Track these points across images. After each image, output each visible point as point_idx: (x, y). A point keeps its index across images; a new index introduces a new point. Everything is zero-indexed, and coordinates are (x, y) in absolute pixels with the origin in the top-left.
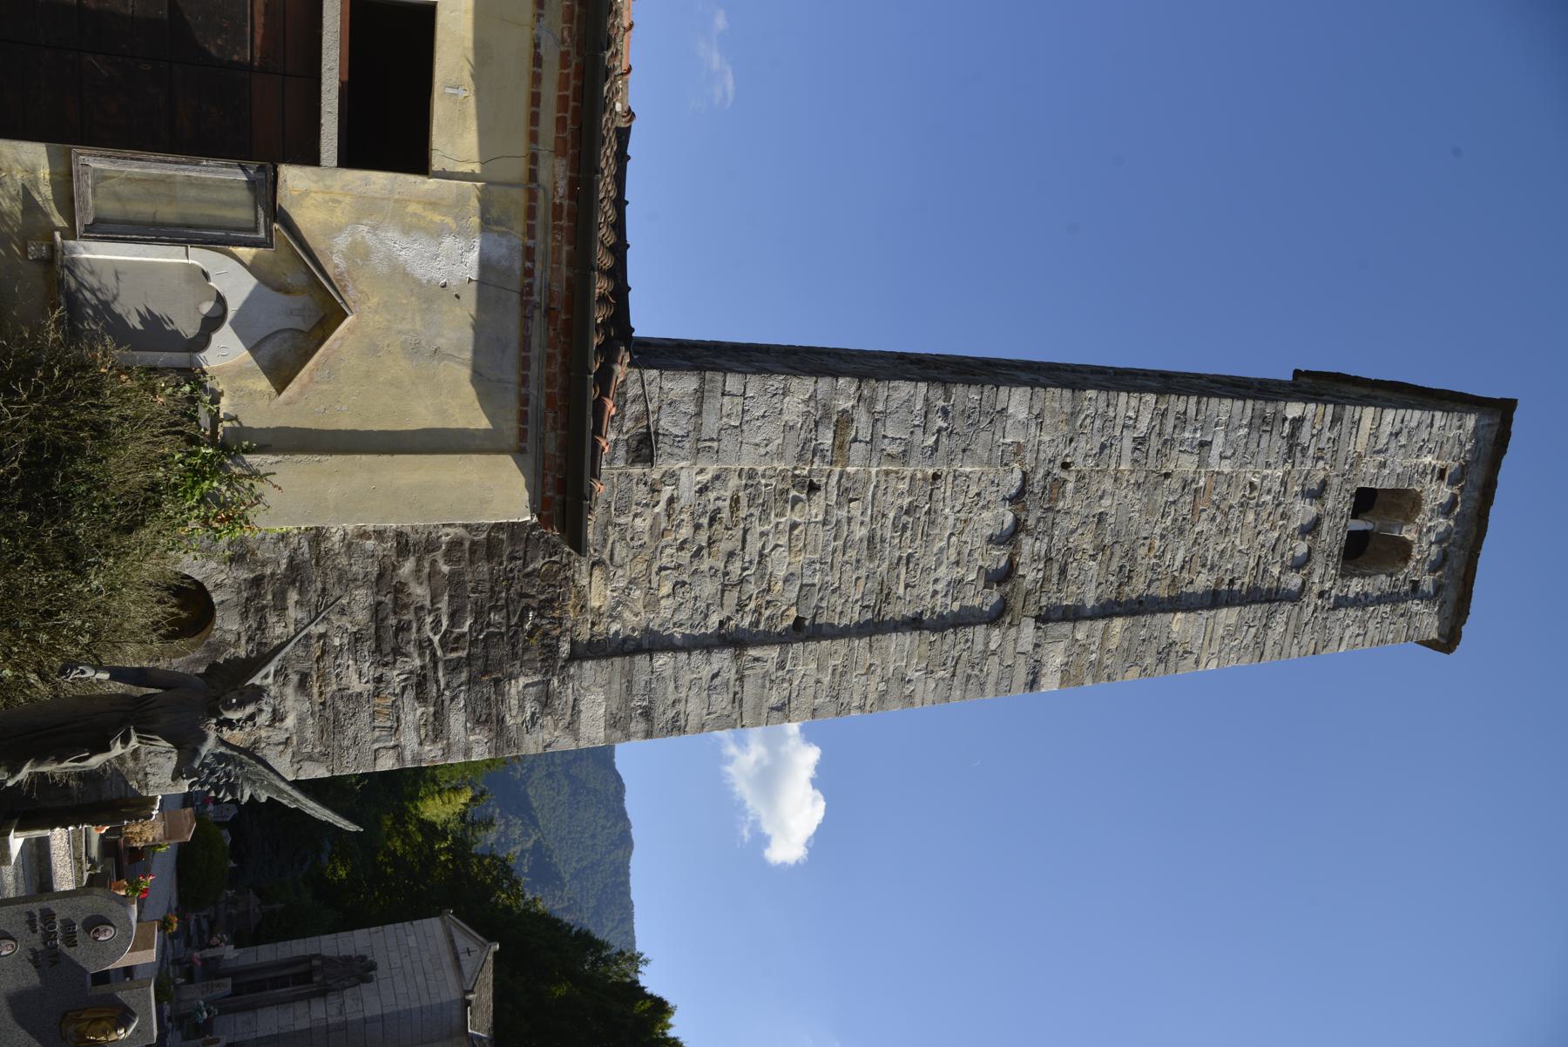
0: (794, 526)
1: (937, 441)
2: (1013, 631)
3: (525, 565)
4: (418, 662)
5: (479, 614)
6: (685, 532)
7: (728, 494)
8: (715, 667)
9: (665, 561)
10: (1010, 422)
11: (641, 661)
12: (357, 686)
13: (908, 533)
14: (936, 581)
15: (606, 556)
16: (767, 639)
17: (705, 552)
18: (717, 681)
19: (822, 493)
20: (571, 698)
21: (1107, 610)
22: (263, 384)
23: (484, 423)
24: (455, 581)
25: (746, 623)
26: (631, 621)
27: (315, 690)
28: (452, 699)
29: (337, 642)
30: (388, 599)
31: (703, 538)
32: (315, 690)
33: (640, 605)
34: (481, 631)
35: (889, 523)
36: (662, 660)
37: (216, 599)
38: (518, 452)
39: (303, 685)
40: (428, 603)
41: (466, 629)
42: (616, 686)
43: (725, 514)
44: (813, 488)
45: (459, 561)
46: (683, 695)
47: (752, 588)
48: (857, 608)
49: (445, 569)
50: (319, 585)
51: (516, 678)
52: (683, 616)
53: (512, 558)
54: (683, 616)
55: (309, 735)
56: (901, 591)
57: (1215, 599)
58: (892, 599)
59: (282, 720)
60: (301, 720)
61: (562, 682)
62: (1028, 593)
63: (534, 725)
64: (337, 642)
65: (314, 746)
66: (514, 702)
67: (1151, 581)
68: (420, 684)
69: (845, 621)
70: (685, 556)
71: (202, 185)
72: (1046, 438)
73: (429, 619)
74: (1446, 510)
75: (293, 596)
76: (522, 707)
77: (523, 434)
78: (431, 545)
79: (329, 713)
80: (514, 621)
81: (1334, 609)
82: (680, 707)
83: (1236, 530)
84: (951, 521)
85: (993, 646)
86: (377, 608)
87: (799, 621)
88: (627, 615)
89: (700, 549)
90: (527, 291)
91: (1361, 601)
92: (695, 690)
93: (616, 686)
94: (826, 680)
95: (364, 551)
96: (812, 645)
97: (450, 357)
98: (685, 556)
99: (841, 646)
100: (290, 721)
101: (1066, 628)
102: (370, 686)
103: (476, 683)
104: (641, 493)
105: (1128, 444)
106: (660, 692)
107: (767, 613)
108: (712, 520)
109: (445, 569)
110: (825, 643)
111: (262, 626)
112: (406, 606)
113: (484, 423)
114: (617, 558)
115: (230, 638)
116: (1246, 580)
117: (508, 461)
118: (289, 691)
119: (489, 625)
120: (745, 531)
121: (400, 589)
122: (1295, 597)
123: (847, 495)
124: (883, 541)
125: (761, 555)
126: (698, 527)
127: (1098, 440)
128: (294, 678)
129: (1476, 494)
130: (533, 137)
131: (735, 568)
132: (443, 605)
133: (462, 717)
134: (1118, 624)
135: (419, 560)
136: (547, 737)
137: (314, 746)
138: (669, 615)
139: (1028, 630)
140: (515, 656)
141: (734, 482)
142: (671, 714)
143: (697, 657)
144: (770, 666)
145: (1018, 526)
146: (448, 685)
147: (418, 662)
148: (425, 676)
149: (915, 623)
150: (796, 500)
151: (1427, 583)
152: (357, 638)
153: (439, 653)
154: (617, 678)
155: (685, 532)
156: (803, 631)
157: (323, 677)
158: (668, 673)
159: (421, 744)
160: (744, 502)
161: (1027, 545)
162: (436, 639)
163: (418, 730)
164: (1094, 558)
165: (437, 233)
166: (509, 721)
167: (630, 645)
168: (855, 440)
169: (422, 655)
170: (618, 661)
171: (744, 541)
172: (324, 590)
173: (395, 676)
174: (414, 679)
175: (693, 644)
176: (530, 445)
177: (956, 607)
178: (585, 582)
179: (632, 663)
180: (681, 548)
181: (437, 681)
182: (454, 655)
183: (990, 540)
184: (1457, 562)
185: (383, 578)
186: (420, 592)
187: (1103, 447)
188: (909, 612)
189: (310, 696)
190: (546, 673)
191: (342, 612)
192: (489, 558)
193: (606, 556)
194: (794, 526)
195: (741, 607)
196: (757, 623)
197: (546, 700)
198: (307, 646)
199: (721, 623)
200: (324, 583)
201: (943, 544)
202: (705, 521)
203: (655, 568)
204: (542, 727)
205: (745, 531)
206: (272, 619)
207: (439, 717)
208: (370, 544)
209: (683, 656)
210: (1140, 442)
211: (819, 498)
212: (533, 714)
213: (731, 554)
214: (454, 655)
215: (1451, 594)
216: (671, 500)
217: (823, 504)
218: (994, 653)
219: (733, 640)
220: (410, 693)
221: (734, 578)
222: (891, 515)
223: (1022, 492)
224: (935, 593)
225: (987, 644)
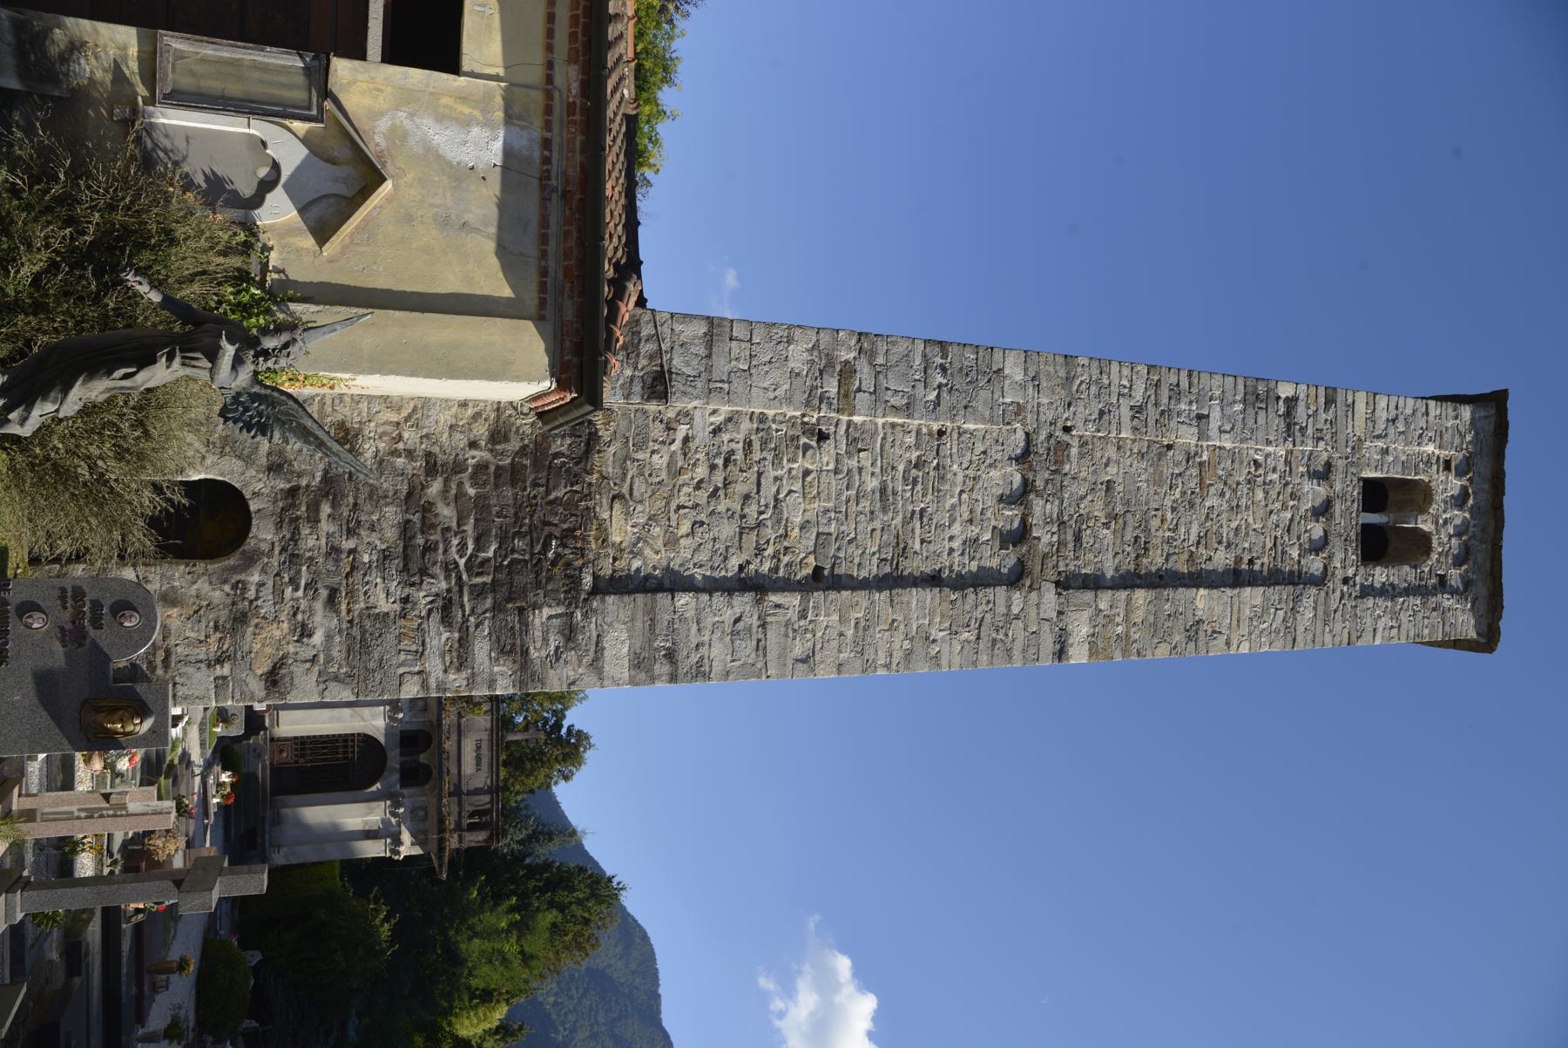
0: (807, 473)
1: (938, 396)
2: (1034, 594)
3: (548, 492)
4: (444, 585)
5: (503, 539)
6: (701, 471)
7: (741, 437)
8: (738, 611)
9: (683, 500)
10: (1007, 382)
11: (663, 599)
12: (384, 605)
13: (919, 487)
14: (951, 538)
15: (625, 490)
16: (787, 586)
17: (721, 492)
18: (740, 626)
19: (831, 441)
20: (594, 634)
21: (1129, 581)
22: (309, 242)
23: (507, 292)
24: (481, 504)
25: (765, 568)
26: (651, 559)
27: (344, 607)
28: (477, 626)
29: (366, 558)
30: (416, 518)
31: (718, 478)
32: (344, 607)
33: (660, 543)
34: (506, 557)
35: (900, 475)
36: (683, 599)
37: (253, 507)
38: (539, 319)
39: (332, 601)
40: (454, 525)
41: (491, 554)
42: (639, 624)
43: (739, 456)
44: (822, 437)
45: (485, 484)
46: (706, 638)
47: (769, 532)
48: (875, 561)
49: (472, 492)
50: (351, 500)
51: (540, 608)
52: (703, 556)
53: (535, 485)
54: (703, 556)
55: (335, 653)
56: (917, 546)
57: (1236, 578)
58: (910, 555)
59: (310, 636)
60: (329, 637)
61: (585, 616)
62: (1045, 556)
63: (558, 660)
64: (366, 558)
65: (340, 666)
66: (538, 634)
67: (1169, 555)
68: (445, 608)
69: (864, 574)
70: (702, 496)
71: (265, 68)
72: (1045, 401)
73: (455, 542)
74: (1460, 501)
75: (326, 509)
76: (545, 640)
77: (542, 303)
78: (458, 467)
79: (356, 632)
80: (538, 548)
81: (1362, 597)
82: (704, 651)
83: (1247, 508)
84: (960, 478)
85: (1015, 610)
86: (405, 528)
87: (818, 570)
88: (648, 552)
89: (717, 489)
90: (545, 177)
91: (1389, 592)
92: (718, 634)
93: (639, 624)
94: (850, 633)
95: (394, 469)
96: (833, 595)
97: (477, 231)
98: (702, 496)
99: (861, 597)
100: (318, 638)
101: (1088, 596)
102: (397, 607)
103: (500, 611)
104: (657, 431)
105: (1126, 413)
106: (683, 633)
107: (786, 559)
108: (727, 461)
109: (472, 492)
110: (845, 594)
111: (295, 538)
112: (433, 526)
113: (507, 292)
114: (636, 493)
115: (265, 547)
116: (1266, 560)
117: (530, 325)
118: (319, 605)
119: (513, 551)
120: (760, 474)
121: (428, 508)
122: (1320, 581)
123: (855, 443)
124: (895, 493)
125: (776, 499)
126: (713, 467)
127: (1096, 407)
128: (324, 593)
129: (1486, 487)
130: (549, 48)
131: (752, 510)
132: (469, 527)
133: (486, 645)
134: (1141, 596)
135: (446, 481)
136: (571, 673)
137: (340, 666)
138: (688, 556)
139: (1049, 596)
140: (538, 585)
141: (746, 425)
142: (694, 658)
143: (719, 599)
144: (792, 614)
145: (1027, 487)
146: (473, 611)
147: (444, 585)
148: (450, 600)
149: (933, 580)
150: (806, 448)
151: (1454, 576)
152: (385, 556)
153: (465, 577)
154: (640, 615)
155: (701, 471)
156: (821, 581)
157: (351, 593)
158: (690, 614)
159: (445, 671)
160: (756, 445)
161: (1039, 507)
162: (462, 562)
163: (443, 656)
164: (1106, 525)
165: (466, 123)
166: (534, 654)
167: (651, 584)
168: (859, 390)
169: (447, 578)
170: (640, 597)
171: (759, 484)
172: (355, 504)
173: (422, 598)
174: (440, 603)
175: (712, 586)
176: (549, 312)
177: (974, 566)
178: (605, 515)
179: (654, 601)
180: (698, 487)
181: (462, 606)
182: (479, 580)
183: (1001, 499)
184: (1481, 556)
185: (412, 497)
186: (447, 513)
187: (1101, 413)
188: (927, 568)
189: (338, 612)
190: (569, 605)
191: (372, 528)
192: (513, 483)
193: (625, 490)
194: (807, 473)
195: (759, 551)
196: (776, 569)
197: (570, 633)
198: (337, 561)
199: (741, 568)
200: (356, 498)
201: (955, 500)
202: (720, 462)
203: (673, 506)
204: (566, 662)
205: (760, 474)
206: (305, 531)
207: (464, 642)
208: (400, 461)
209: (705, 597)
210: (1138, 410)
211: (828, 445)
212: (557, 648)
213: (747, 497)
214: (479, 580)
215: (1482, 590)
216: (686, 440)
217: (833, 452)
218: (1017, 618)
219: (755, 586)
220: (436, 617)
221: (751, 521)
222: (901, 468)
223: (1027, 452)
224: (951, 550)
225: (1009, 607)
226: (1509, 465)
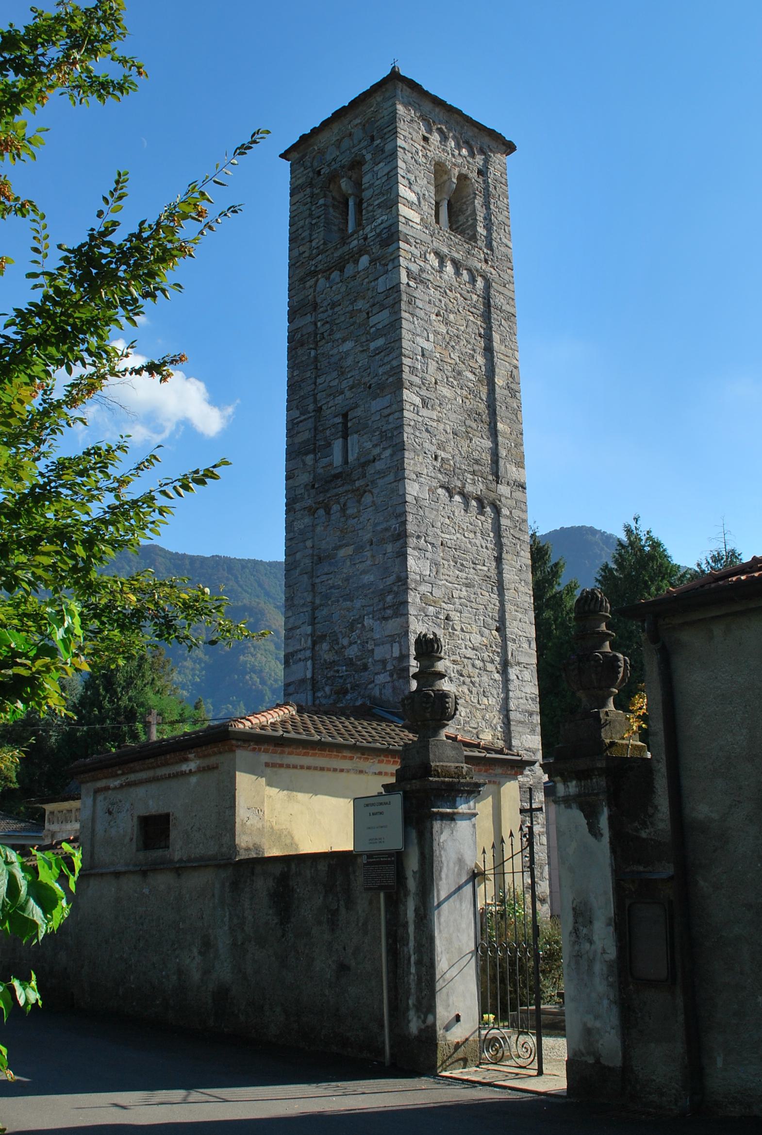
1: (430, 543)
2: (503, 499)
7: (452, 665)
9: (476, 701)
10: (420, 495)
11: (513, 715)
14: (482, 547)
15: (475, 731)
16: (504, 648)
17: (473, 680)
19: (450, 613)
21: (494, 433)
23: (490, 799)
25: (498, 659)
26: (497, 719)
31: (468, 680)
33: (491, 715)
35: (460, 574)
36: (512, 706)
38: (500, 785)
43: (458, 667)
44: (448, 618)
46: (524, 694)
47: (485, 655)
48: (492, 595)
52: (495, 692)
54: (495, 692)
56: (485, 568)
57: (489, 350)
58: (489, 574)
62: (487, 488)
67: (480, 398)
69: (498, 604)
70: (474, 690)
72: (425, 472)
77: (494, 782)
81: (492, 250)
83: (458, 329)
84: (458, 535)
87: (497, 630)
89: (471, 682)
91: (489, 227)
92: (523, 689)
94: (520, 616)
96: (508, 624)
99: (508, 606)
101: (501, 463)
105: (424, 412)
106: (523, 707)
108: (462, 675)
110: (507, 617)
113: (490, 799)
114: (475, 726)
116: (479, 323)
117: (502, 789)
120: (465, 657)
122: (488, 286)
123: (450, 599)
124: (467, 578)
125: (473, 649)
126: (464, 683)
127: (426, 435)
129: (437, 110)
131: (478, 663)
134: (500, 426)
138: (493, 701)
139: (504, 489)
143: (511, 687)
144: (515, 647)
145: (462, 494)
149: (499, 560)
151: (479, 159)
156: (501, 629)
161: (469, 488)
164: (471, 440)
167: (505, 721)
168: (431, 593)
170: (512, 728)
171: (468, 658)
175: (506, 690)
176: (497, 780)
177: (492, 535)
179: (513, 721)
180: (471, 692)
183: (466, 511)
184: (470, 132)
187: (427, 430)
188: (494, 564)
193: (475, 731)
195: (492, 662)
196: (498, 652)
199: (498, 672)
202: (462, 679)
203: (478, 706)
205: (465, 657)
209: (511, 693)
210: (425, 404)
213: (473, 666)
215: (486, 140)
217: (454, 613)
218: (511, 513)
219: (505, 665)
221: (481, 664)
222: (458, 572)
223: (448, 489)
224: (487, 548)
226: (432, 92)
